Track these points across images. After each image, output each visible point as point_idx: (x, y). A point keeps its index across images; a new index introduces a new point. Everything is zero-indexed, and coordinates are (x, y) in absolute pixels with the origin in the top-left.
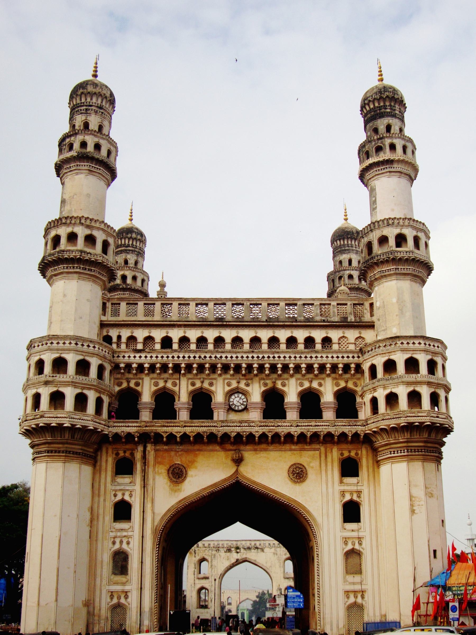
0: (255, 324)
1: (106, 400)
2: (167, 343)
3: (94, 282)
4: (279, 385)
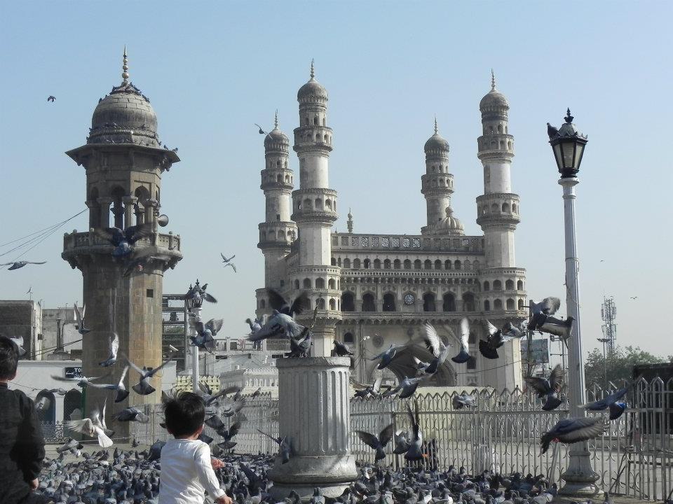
2: (367, 262)
4: (432, 289)
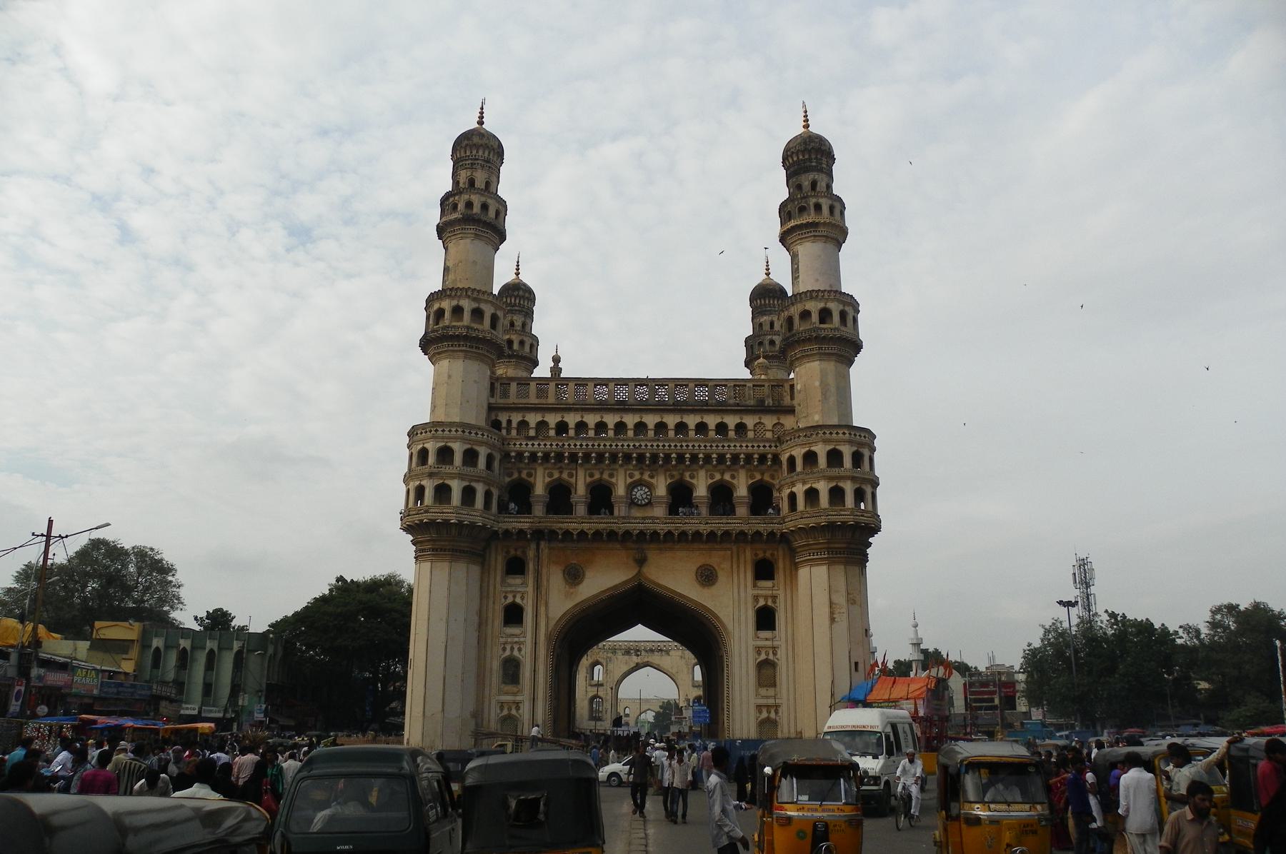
0: (661, 408)
1: (495, 492)
2: (562, 428)
3: (482, 361)
